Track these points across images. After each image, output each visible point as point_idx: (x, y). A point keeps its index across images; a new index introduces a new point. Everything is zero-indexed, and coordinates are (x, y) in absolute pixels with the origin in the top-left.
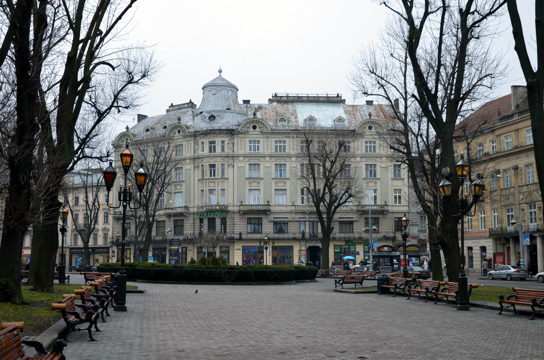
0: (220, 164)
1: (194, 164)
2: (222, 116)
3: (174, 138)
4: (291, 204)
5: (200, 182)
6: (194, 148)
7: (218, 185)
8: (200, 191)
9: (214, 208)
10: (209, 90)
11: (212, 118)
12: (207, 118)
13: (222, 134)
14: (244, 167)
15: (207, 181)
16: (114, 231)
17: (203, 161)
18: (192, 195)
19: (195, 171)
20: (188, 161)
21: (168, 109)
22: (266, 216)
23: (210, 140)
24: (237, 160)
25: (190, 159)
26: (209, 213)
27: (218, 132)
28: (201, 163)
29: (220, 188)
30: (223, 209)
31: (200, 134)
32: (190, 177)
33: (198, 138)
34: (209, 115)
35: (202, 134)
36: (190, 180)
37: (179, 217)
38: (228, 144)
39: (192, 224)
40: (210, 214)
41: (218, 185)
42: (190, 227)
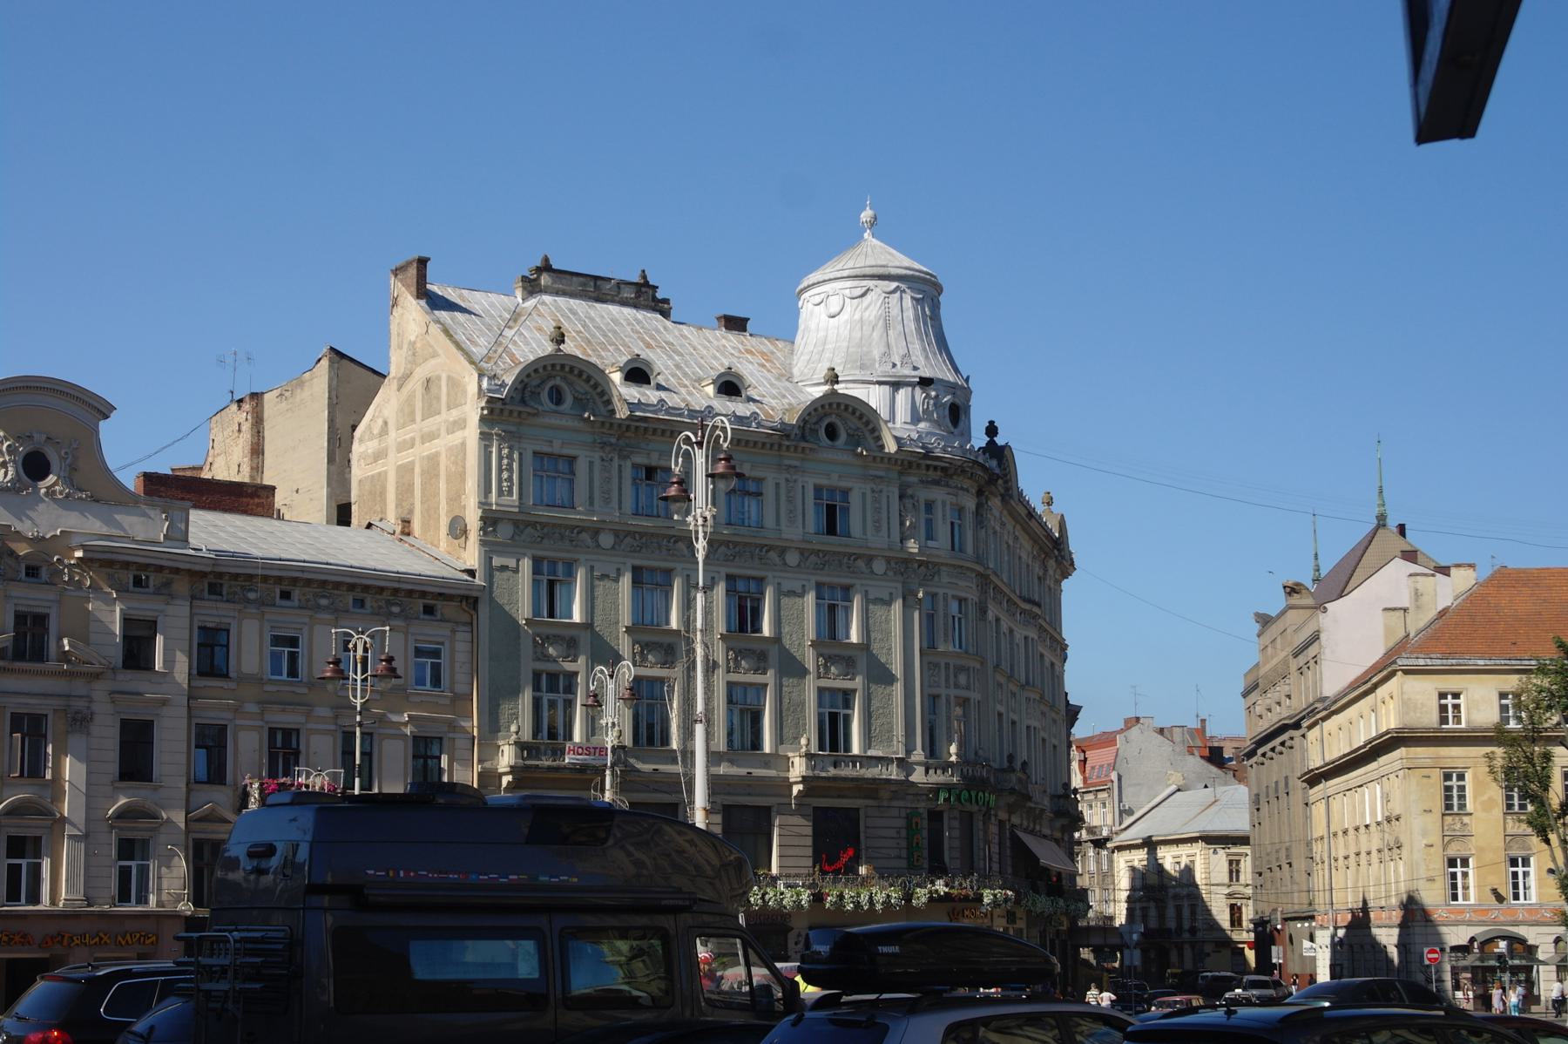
1: (904, 583)
17: (936, 578)
26: (973, 794)
31: (928, 467)
39: (904, 833)
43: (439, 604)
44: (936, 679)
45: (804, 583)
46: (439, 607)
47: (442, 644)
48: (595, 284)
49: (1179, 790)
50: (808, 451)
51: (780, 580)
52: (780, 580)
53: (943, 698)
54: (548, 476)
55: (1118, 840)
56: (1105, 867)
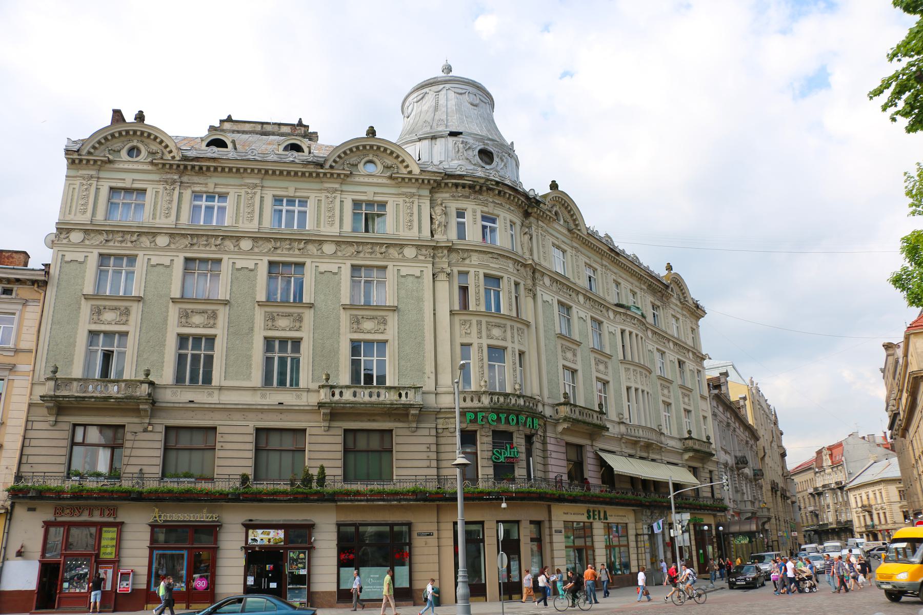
0: (513, 279)
2: (505, 160)
3: (349, 179)
4: (617, 420)
5: (457, 319)
6: (431, 219)
7: (513, 337)
8: (458, 349)
9: (513, 401)
10: (460, 91)
11: (486, 155)
12: (476, 152)
13: (510, 204)
14: (551, 305)
15: (484, 320)
16: (27, 451)
17: (467, 261)
18: (430, 355)
19: (438, 284)
20: (410, 252)
21: (217, 124)
22: (589, 442)
23: (485, 209)
24: (541, 283)
25: (418, 247)
26: (503, 416)
27: (510, 195)
28: (457, 265)
29: (517, 347)
30: (531, 408)
31: (456, 185)
32: (420, 300)
33: (447, 195)
34: (481, 147)
35: (464, 186)
36: (420, 311)
37: (374, 421)
38: (525, 233)
39: (434, 448)
40: (507, 419)
41: (513, 337)
42: (424, 456)
43: (15, 287)
44: (469, 332)
45: (340, 265)
46: (15, 289)
47: (14, 314)
48: (262, 127)
49: (875, 462)
50: (342, 176)
51: (317, 264)
52: (317, 264)
53: (475, 346)
54: (123, 203)
55: (849, 486)
56: (845, 499)
